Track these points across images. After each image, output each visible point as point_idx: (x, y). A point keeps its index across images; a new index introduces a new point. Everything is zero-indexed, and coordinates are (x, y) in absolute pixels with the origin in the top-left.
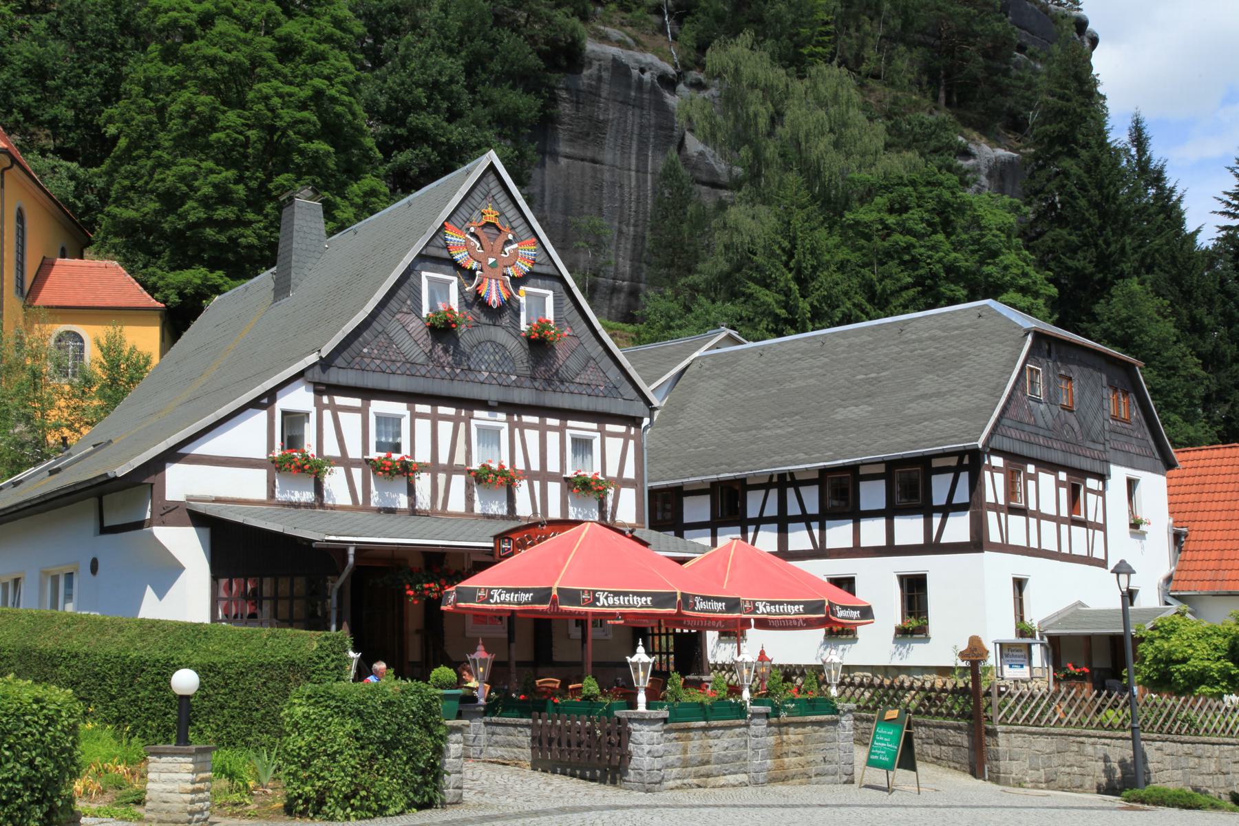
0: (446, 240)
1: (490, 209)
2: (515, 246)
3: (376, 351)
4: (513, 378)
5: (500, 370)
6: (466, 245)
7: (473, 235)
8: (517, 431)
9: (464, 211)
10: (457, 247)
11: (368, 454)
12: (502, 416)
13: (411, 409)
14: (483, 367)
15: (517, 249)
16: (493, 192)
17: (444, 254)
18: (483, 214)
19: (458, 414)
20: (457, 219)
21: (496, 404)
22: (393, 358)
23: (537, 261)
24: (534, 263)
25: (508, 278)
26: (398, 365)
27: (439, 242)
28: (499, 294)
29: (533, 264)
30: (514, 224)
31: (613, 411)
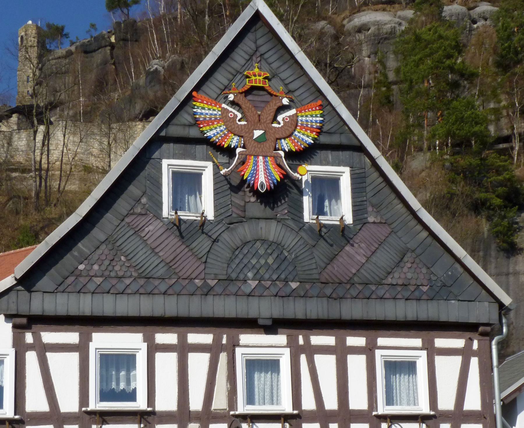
0: (195, 113)
1: (256, 70)
2: (293, 112)
3: (96, 267)
4: (294, 285)
5: (275, 277)
6: (224, 117)
7: (233, 104)
8: (303, 358)
9: (221, 77)
10: (210, 122)
11: (87, 405)
12: (281, 339)
13: (149, 340)
14: (250, 275)
15: (296, 115)
16: (262, 50)
17: (193, 133)
18: (247, 77)
19: (217, 340)
20: (211, 88)
21: (269, 323)
22: (121, 274)
23: (325, 129)
24: (320, 131)
25: (282, 153)
26: (128, 281)
27: (185, 117)
28: (268, 174)
29: (318, 134)
30: (292, 87)
31: (443, 318)
